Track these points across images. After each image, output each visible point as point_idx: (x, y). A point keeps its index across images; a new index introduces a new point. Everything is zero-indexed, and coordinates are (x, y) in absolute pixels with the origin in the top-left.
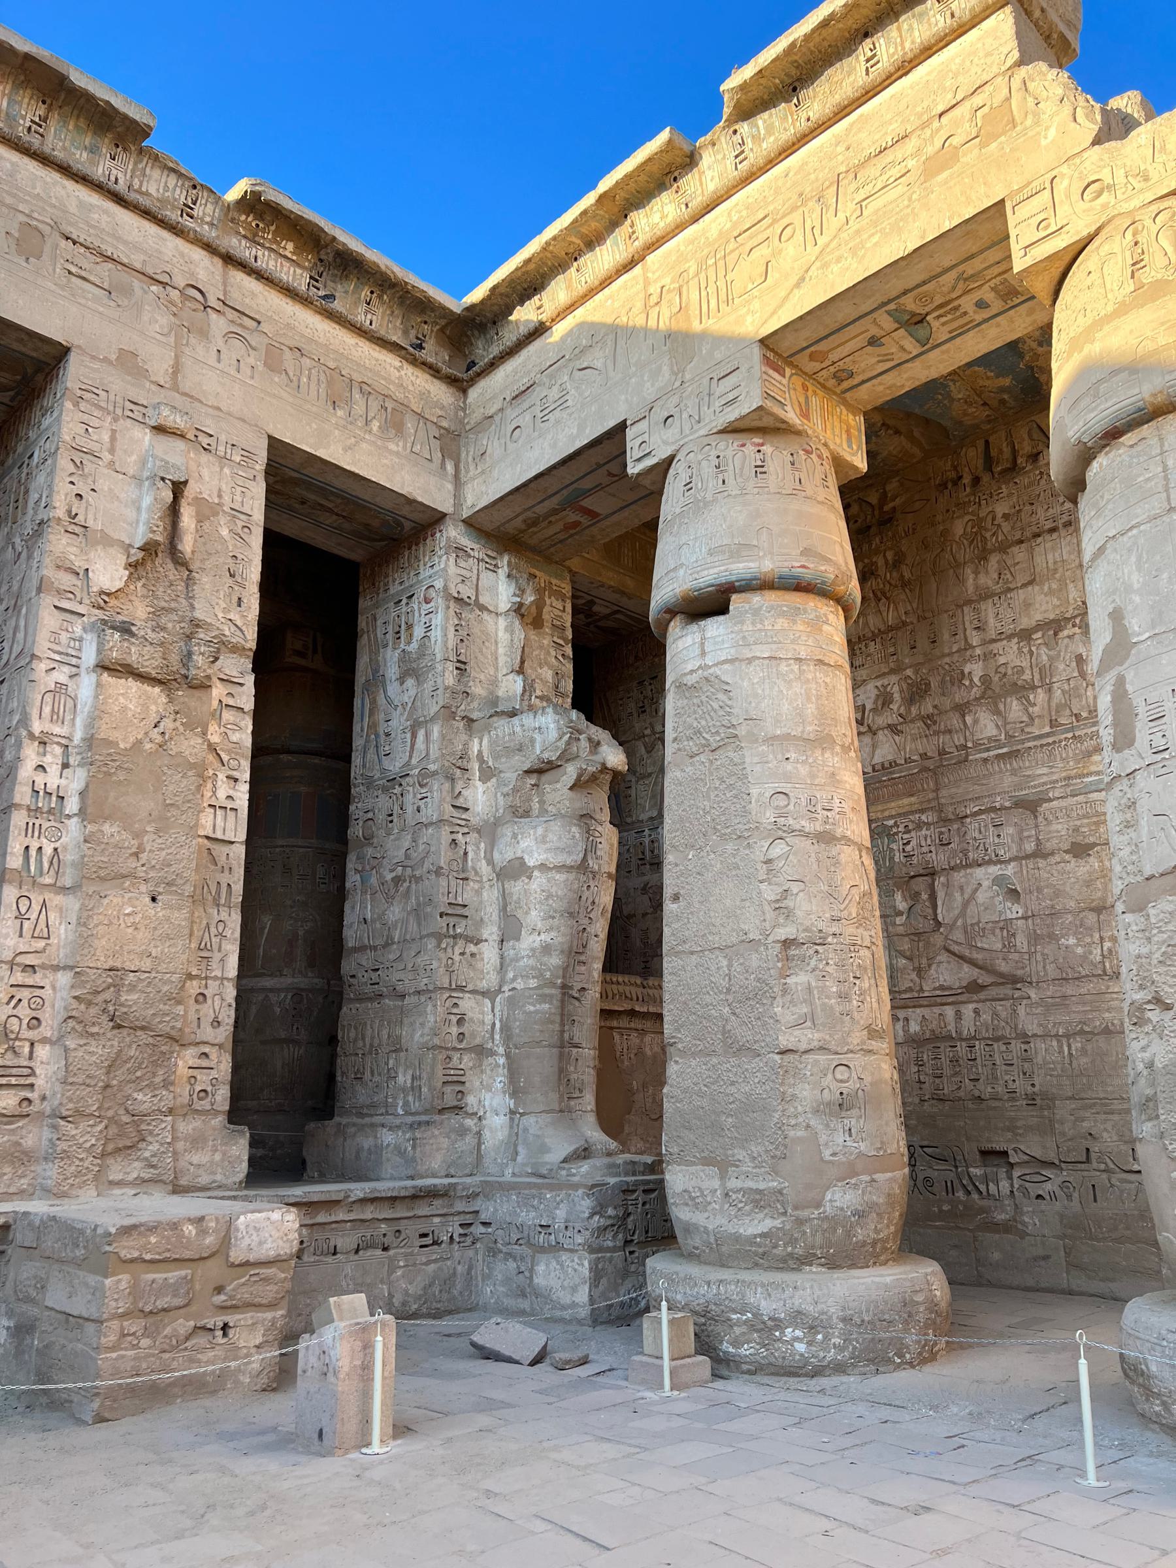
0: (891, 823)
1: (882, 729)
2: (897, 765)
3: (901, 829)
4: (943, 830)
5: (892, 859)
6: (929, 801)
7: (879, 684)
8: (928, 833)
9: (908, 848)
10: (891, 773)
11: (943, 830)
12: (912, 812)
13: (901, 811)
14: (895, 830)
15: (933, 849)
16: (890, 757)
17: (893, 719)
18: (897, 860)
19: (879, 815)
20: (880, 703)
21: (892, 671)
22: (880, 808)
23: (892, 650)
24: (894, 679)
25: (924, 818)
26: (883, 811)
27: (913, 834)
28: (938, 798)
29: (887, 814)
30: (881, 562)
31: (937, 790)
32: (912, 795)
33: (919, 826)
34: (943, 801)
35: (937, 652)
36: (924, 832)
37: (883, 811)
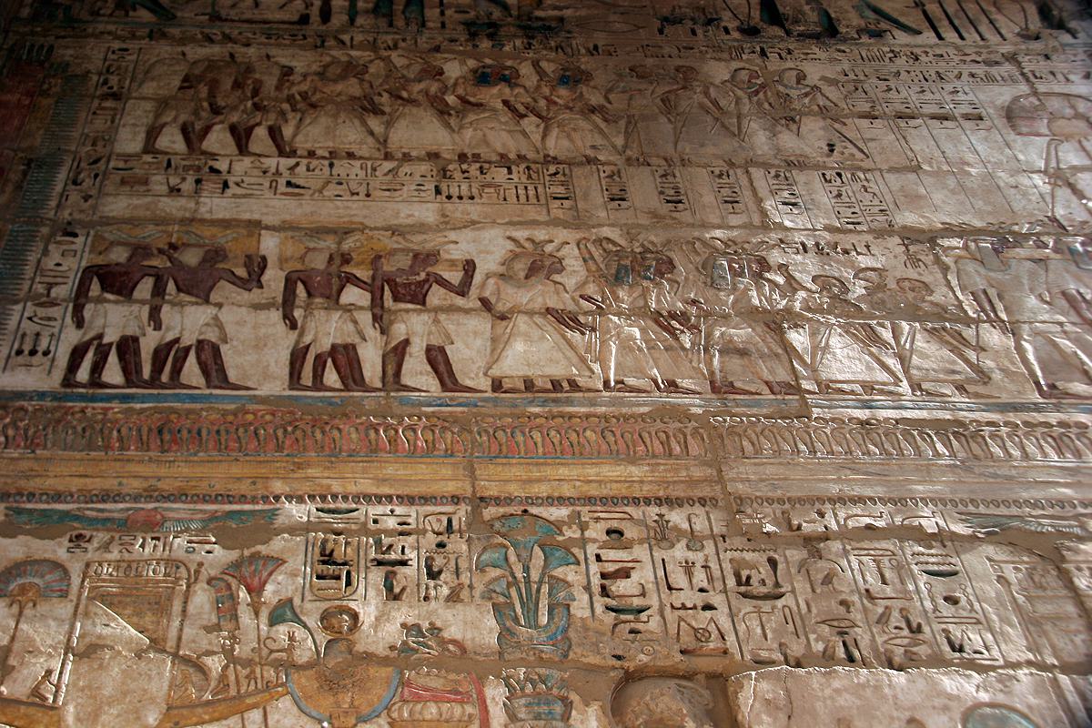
0: (560, 513)
1: (531, 313)
2: (574, 386)
3: (596, 532)
4: (748, 556)
5: (560, 607)
6: (692, 483)
7: (520, 234)
8: (698, 557)
9: (620, 586)
10: (555, 401)
11: (748, 556)
12: (636, 501)
13: (594, 491)
14: (572, 533)
15: (717, 599)
16: (558, 371)
17: (565, 302)
18: (580, 608)
19: (515, 490)
20: (521, 267)
21: (556, 223)
22: (518, 471)
23: (560, 190)
24: (562, 234)
25: (677, 517)
26: (530, 481)
27: (640, 552)
28: (720, 480)
29: (543, 490)
30: (526, 70)
31: (717, 464)
32: (633, 461)
33: (661, 535)
34: (741, 488)
35: (686, 217)
36: (680, 552)
37: (530, 481)
